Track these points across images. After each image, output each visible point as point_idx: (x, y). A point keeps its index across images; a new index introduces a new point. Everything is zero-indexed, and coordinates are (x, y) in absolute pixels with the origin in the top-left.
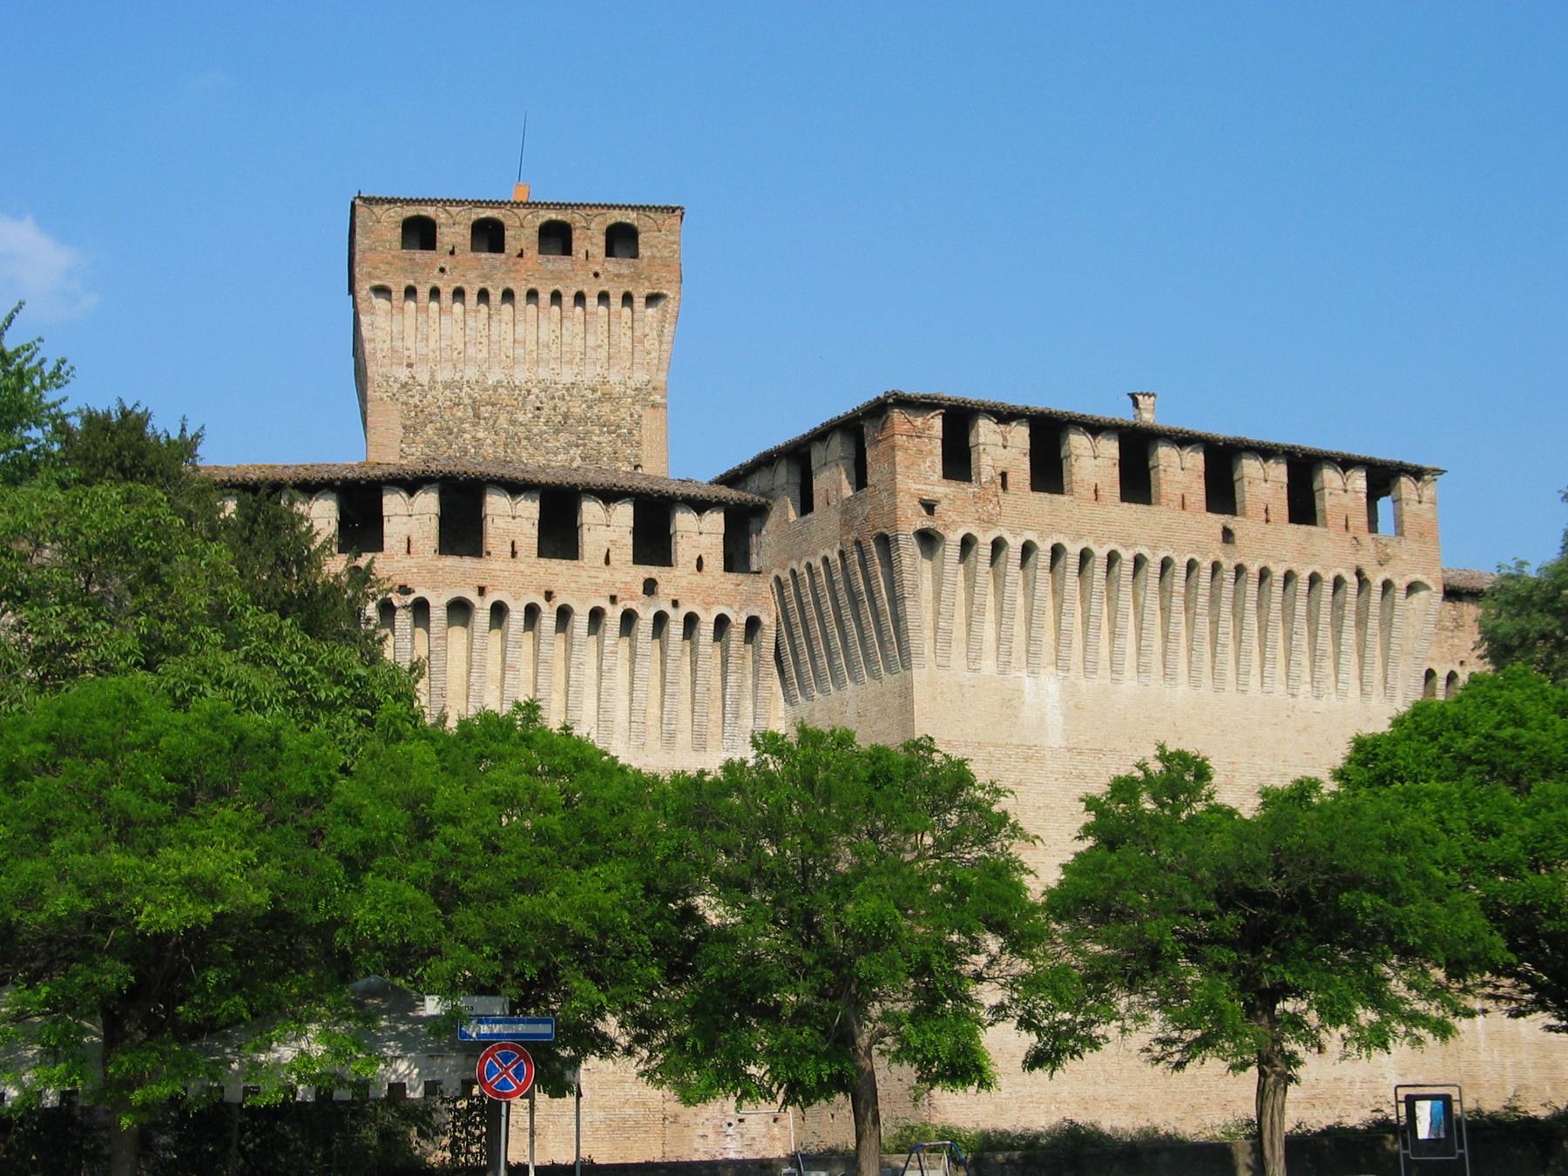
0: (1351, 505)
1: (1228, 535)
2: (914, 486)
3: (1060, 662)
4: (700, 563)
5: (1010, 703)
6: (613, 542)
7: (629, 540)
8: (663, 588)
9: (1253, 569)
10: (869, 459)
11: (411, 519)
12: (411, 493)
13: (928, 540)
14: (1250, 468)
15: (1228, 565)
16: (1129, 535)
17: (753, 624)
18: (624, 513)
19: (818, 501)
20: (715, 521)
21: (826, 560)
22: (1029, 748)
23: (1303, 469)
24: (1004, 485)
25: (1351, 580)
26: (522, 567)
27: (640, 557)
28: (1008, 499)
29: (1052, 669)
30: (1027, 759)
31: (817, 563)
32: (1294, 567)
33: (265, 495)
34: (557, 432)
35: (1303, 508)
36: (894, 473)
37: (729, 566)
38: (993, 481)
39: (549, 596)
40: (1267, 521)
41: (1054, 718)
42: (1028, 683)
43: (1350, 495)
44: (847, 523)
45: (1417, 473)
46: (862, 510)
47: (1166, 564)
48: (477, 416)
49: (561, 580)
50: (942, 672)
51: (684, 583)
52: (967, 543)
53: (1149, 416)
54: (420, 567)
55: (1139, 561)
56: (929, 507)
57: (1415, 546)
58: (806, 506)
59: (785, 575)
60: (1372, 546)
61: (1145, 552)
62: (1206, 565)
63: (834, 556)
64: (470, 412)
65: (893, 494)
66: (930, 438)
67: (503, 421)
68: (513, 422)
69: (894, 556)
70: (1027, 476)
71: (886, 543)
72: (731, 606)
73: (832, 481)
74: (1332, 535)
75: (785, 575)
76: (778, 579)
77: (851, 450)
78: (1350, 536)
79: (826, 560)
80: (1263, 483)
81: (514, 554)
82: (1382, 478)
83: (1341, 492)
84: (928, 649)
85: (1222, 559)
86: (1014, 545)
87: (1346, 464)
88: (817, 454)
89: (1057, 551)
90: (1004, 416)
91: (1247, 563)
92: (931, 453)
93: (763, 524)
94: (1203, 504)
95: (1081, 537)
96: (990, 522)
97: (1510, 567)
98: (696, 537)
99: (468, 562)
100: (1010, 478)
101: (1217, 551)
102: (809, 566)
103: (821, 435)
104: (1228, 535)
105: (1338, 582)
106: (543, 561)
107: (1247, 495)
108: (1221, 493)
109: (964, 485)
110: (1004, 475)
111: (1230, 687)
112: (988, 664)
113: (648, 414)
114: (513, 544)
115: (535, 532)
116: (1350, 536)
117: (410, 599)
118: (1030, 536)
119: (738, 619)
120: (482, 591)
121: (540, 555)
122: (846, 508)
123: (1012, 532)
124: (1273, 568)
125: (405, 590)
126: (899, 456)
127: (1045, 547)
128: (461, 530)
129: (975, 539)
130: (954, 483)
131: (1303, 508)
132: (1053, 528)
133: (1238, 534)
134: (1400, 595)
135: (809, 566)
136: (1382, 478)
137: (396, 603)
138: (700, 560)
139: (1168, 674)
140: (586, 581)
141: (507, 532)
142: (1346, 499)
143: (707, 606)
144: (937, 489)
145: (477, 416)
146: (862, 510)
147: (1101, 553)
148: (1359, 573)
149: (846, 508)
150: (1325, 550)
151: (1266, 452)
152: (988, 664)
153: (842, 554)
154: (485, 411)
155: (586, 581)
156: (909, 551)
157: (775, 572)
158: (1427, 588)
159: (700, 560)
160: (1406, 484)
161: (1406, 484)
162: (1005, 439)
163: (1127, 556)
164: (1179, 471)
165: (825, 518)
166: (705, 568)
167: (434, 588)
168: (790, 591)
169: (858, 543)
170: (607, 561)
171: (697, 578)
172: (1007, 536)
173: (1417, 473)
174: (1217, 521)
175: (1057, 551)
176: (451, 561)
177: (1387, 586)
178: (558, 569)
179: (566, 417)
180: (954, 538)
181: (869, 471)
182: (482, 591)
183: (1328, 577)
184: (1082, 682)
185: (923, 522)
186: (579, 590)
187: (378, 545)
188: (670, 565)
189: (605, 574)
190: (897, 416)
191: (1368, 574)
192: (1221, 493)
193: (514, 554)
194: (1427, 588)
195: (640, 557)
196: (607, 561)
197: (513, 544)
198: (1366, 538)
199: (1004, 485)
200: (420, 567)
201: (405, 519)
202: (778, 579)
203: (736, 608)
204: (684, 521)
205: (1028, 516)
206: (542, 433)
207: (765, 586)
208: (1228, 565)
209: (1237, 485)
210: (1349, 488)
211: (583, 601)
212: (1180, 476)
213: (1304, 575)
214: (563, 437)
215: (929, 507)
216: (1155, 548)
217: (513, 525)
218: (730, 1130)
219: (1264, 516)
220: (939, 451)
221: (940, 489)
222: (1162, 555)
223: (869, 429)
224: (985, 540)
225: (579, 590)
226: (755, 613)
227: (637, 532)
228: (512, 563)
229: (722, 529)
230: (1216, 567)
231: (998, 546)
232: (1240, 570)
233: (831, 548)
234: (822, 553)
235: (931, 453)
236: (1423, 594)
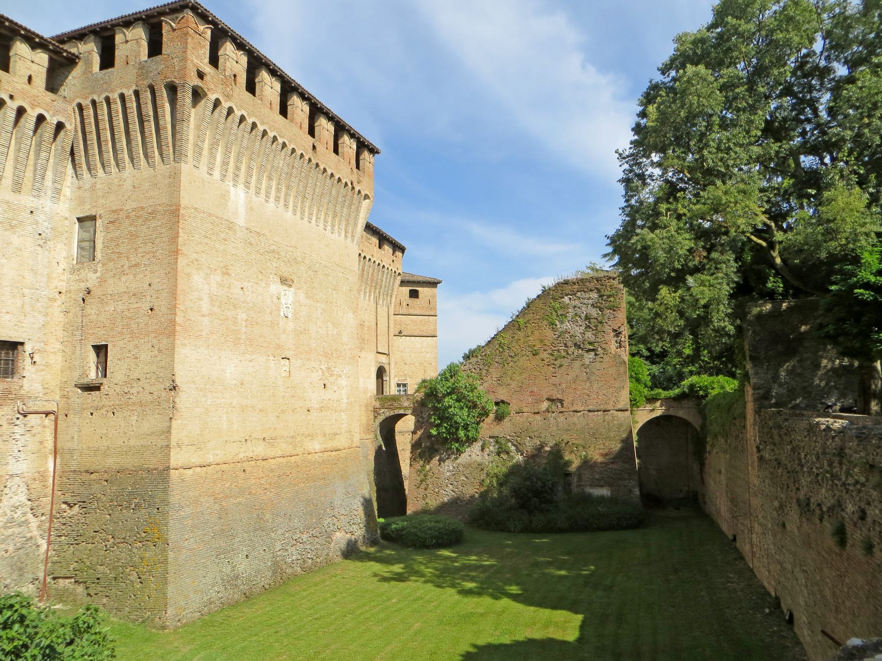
1: (314, 147)
3: (247, 184)
4: (30, 79)
5: (225, 196)
10: (165, 39)
13: (197, 95)
17: (60, 126)
20: (43, 58)
21: (122, 97)
22: (231, 223)
29: (242, 186)
30: (229, 229)
31: (115, 96)
41: (242, 211)
42: (232, 189)
50: (195, 170)
51: (19, 87)
56: (201, 75)
59: (86, 103)
61: (287, 142)
63: (129, 93)
65: (184, 59)
69: (179, 95)
71: (172, 89)
72: (48, 111)
75: (86, 103)
79: (122, 97)
84: (190, 153)
93: (70, 72)
96: (228, 97)
98: (29, 63)
100: (238, 78)
104: (314, 147)
110: (235, 76)
111: (306, 219)
112: (217, 174)
119: (52, 120)
126: (189, 40)
129: (220, 103)
136: (363, 146)
138: (30, 78)
139: (286, 206)
143: (33, 106)
152: (217, 174)
153: (137, 93)
156: (185, 97)
158: (369, 198)
159: (30, 78)
160: (366, 155)
168: (89, 112)
171: (27, 87)
180: (212, 97)
183: (344, 181)
184: (254, 196)
185: (197, 82)
194: (369, 198)
199: (235, 80)
203: (51, 113)
215: (201, 75)
218: (18, 422)
221: (208, 69)
224: (226, 105)
226: (62, 120)
233: (128, 88)
234: (120, 91)
236: (367, 201)
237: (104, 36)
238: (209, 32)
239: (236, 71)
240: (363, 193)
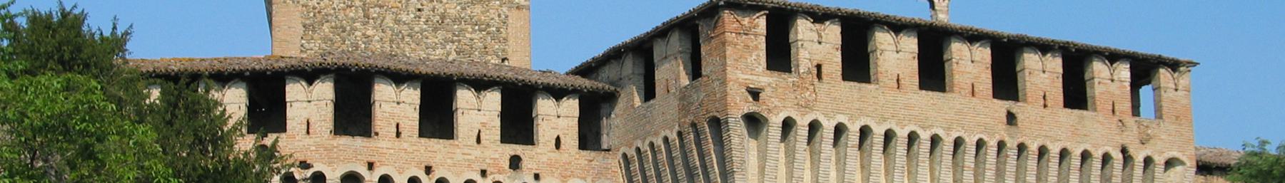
0: (1117, 92)
1: (1011, 118)
2: (742, 76)
6: (484, 124)
7: (498, 122)
8: (526, 163)
9: (1033, 147)
10: (703, 53)
11: (310, 104)
12: (310, 83)
13: (754, 122)
14: (1030, 60)
15: (1012, 144)
16: (927, 119)
18: (493, 99)
19: (659, 89)
20: (571, 106)
21: (666, 140)
23: (1076, 62)
24: (819, 76)
25: (1117, 156)
26: (405, 145)
27: (506, 138)
28: (822, 87)
31: (659, 142)
32: (1068, 145)
33: (185, 83)
34: (435, 30)
35: (1076, 95)
36: (724, 65)
37: (583, 145)
38: (810, 72)
39: (428, 170)
40: (1045, 106)
43: (1116, 84)
44: (684, 108)
45: (1174, 65)
46: (697, 97)
47: (958, 143)
48: (367, 16)
49: (439, 156)
52: (788, 125)
53: (943, 18)
54: (318, 146)
55: (935, 141)
56: (755, 94)
57: (1173, 127)
58: (649, 93)
59: (631, 153)
60: (1135, 128)
61: (941, 133)
62: (992, 144)
63: (673, 136)
64: (361, 13)
65: (724, 83)
66: (756, 35)
67: (389, 21)
68: (397, 21)
70: (839, 68)
71: (717, 124)
73: (672, 72)
74: (1101, 119)
75: (631, 153)
76: (625, 156)
77: (688, 45)
78: (1116, 119)
79: (666, 140)
80: (1042, 74)
81: (398, 134)
82: (1144, 70)
83: (1109, 81)
85: (1007, 139)
86: (828, 126)
87: (1113, 57)
88: (659, 49)
89: (865, 132)
90: (820, 16)
91: (1028, 142)
92: (756, 47)
93: (613, 109)
94: (990, 92)
95: (885, 120)
96: (807, 107)
97: (1254, 145)
98: (554, 119)
99: (359, 141)
101: (1002, 132)
102: (652, 145)
103: (662, 33)
104: (1011, 118)
105: (1106, 159)
106: (423, 140)
107: (1028, 84)
108: (1006, 82)
109: (786, 76)
110: (819, 67)
113: (514, 14)
114: (398, 126)
115: (417, 115)
116: (1116, 119)
117: (309, 173)
118: (842, 119)
120: (371, 166)
121: (421, 135)
122: (684, 95)
123: (826, 115)
124: (1050, 146)
125: (305, 165)
126: (729, 50)
127: (854, 129)
128: (353, 114)
130: (776, 74)
131: (1076, 95)
132: (861, 112)
133: (1020, 117)
134: (1159, 169)
135: (652, 145)
136: (1144, 70)
137: (297, 176)
138: (558, 140)
140: (460, 157)
141: (392, 115)
142: (1113, 87)
144: (762, 79)
145: (367, 16)
146: (697, 97)
147: (902, 133)
148: (1124, 151)
149: (684, 95)
150: (1095, 131)
151: (1044, 47)
153: (680, 134)
154: (374, 12)
155: (460, 157)
156: (737, 132)
157: (623, 150)
158: (1182, 163)
159: (558, 140)
160: (1164, 74)
161: (1164, 74)
162: (820, 36)
163: (925, 136)
164: (969, 64)
165: (665, 104)
166: (562, 146)
167: (330, 164)
168: (635, 166)
169: (694, 125)
170: (479, 141)
171: (555, 155)
172: (822, 119)
173: (1174, 65)
174: (1002, 106)
175: (865, 132)
176: (344, 140)
177: (1148, 161)
178: (437, 146)
179: (443, 17)
180: (776, 120)
181: (704, 63)
182: (371, 166)
185: (750, 107)
186: (454, 165)
187: (281, 127)
188: (533, 144)
189: (477, 152)
190: (727, 16)
191: (1132, 151)
192: (1006, 82)
193: (398, 134)
194: (1182, 163)
195: (506, 138)
196: (479, 141)
197: (398, 126)
198: (1130, 121)
199: (819, 76)
200: (318, 146)
201: (305, 104)
202: (625, 156)
204: (544, 106)
205: (840, 102)
206: (422, 31)
207: (614, 162)
208: (1012, 144)
209: (1019, 75)
210: (1115, 77)
211: (458, 175)
212: (970, 67)
213: (1077, 153)
214: (441, 35)
215: (755, 94)
216: (949, 129)
217: (397, 110)
219: (1042, 102)
220: (764, 46)
222: (955, 135)
223: (703, 28)
224: (803, 122)
225: (454, 165)
227: (504, 115)
228: (397, 143)
229: (577, 113)
230: (1001, 145)
231: (814, 127)
232: (1021, 148)
234: (663, 134)
235: (756, 47)
236: (1179, 168)
237: (642, 51)
238: (761, 22)
239: (818, 59)
240: (1159, 160)
